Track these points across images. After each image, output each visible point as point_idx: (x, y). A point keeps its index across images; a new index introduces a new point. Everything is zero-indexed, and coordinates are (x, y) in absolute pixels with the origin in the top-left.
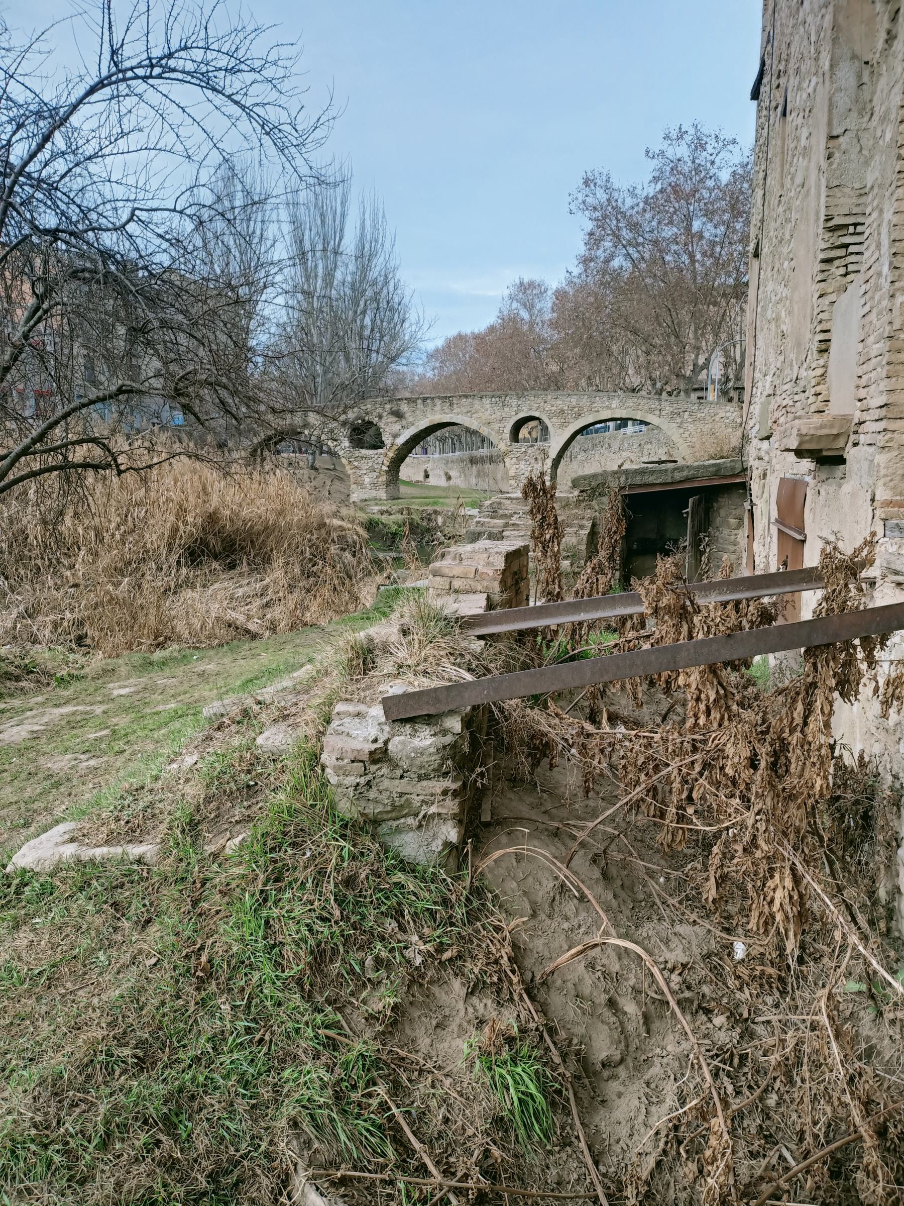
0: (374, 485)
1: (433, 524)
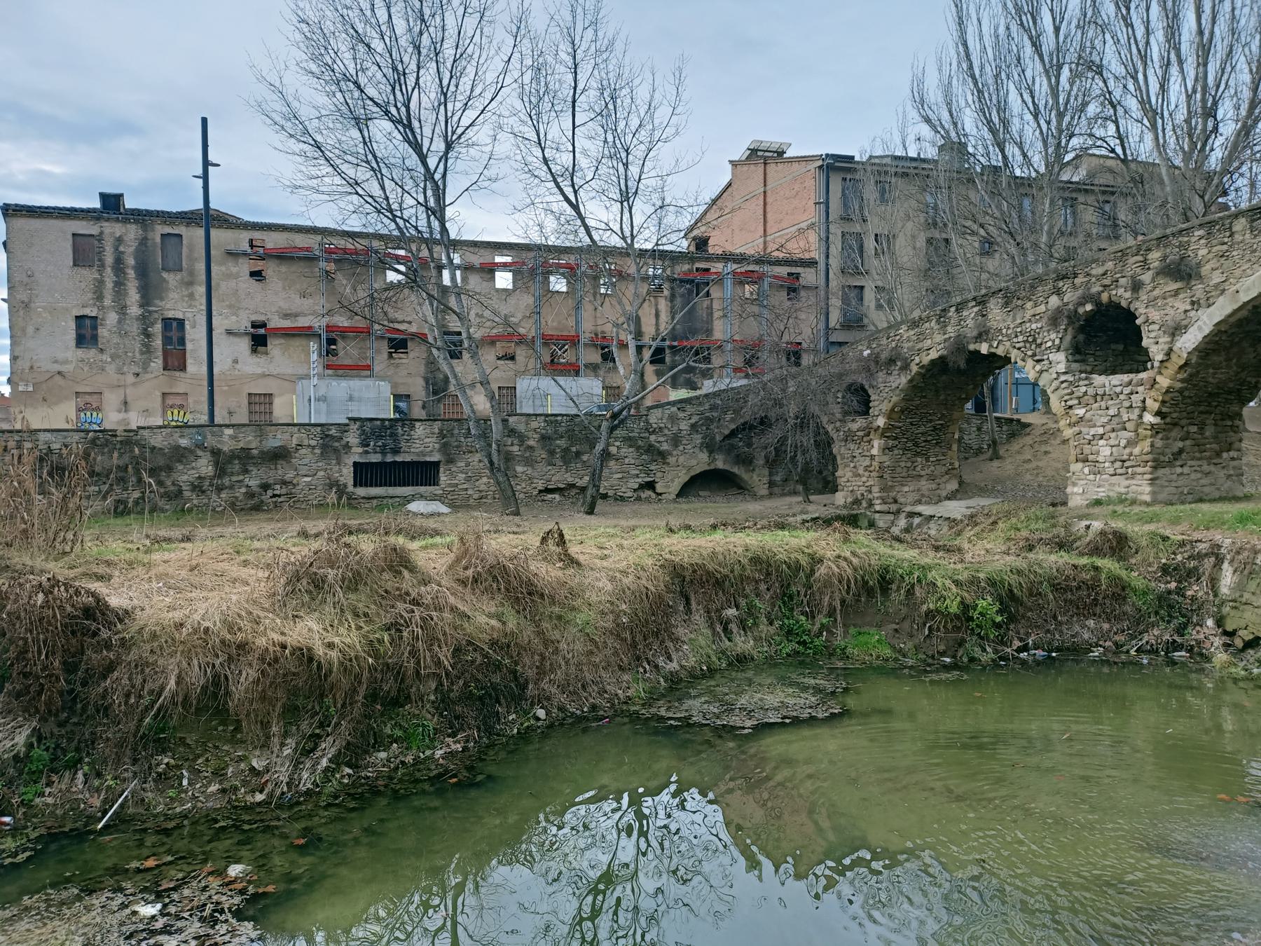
0: (1123, 465)
1: (1196, 590)
